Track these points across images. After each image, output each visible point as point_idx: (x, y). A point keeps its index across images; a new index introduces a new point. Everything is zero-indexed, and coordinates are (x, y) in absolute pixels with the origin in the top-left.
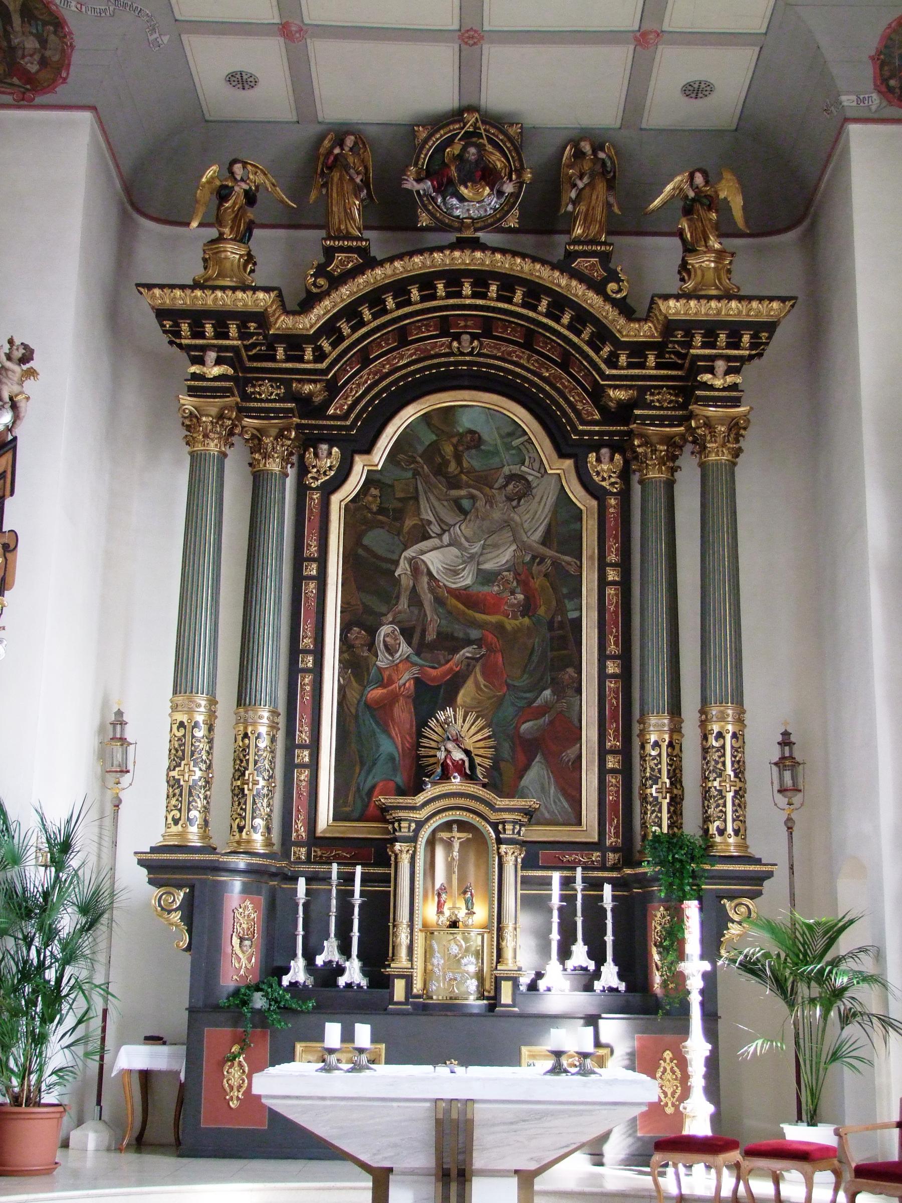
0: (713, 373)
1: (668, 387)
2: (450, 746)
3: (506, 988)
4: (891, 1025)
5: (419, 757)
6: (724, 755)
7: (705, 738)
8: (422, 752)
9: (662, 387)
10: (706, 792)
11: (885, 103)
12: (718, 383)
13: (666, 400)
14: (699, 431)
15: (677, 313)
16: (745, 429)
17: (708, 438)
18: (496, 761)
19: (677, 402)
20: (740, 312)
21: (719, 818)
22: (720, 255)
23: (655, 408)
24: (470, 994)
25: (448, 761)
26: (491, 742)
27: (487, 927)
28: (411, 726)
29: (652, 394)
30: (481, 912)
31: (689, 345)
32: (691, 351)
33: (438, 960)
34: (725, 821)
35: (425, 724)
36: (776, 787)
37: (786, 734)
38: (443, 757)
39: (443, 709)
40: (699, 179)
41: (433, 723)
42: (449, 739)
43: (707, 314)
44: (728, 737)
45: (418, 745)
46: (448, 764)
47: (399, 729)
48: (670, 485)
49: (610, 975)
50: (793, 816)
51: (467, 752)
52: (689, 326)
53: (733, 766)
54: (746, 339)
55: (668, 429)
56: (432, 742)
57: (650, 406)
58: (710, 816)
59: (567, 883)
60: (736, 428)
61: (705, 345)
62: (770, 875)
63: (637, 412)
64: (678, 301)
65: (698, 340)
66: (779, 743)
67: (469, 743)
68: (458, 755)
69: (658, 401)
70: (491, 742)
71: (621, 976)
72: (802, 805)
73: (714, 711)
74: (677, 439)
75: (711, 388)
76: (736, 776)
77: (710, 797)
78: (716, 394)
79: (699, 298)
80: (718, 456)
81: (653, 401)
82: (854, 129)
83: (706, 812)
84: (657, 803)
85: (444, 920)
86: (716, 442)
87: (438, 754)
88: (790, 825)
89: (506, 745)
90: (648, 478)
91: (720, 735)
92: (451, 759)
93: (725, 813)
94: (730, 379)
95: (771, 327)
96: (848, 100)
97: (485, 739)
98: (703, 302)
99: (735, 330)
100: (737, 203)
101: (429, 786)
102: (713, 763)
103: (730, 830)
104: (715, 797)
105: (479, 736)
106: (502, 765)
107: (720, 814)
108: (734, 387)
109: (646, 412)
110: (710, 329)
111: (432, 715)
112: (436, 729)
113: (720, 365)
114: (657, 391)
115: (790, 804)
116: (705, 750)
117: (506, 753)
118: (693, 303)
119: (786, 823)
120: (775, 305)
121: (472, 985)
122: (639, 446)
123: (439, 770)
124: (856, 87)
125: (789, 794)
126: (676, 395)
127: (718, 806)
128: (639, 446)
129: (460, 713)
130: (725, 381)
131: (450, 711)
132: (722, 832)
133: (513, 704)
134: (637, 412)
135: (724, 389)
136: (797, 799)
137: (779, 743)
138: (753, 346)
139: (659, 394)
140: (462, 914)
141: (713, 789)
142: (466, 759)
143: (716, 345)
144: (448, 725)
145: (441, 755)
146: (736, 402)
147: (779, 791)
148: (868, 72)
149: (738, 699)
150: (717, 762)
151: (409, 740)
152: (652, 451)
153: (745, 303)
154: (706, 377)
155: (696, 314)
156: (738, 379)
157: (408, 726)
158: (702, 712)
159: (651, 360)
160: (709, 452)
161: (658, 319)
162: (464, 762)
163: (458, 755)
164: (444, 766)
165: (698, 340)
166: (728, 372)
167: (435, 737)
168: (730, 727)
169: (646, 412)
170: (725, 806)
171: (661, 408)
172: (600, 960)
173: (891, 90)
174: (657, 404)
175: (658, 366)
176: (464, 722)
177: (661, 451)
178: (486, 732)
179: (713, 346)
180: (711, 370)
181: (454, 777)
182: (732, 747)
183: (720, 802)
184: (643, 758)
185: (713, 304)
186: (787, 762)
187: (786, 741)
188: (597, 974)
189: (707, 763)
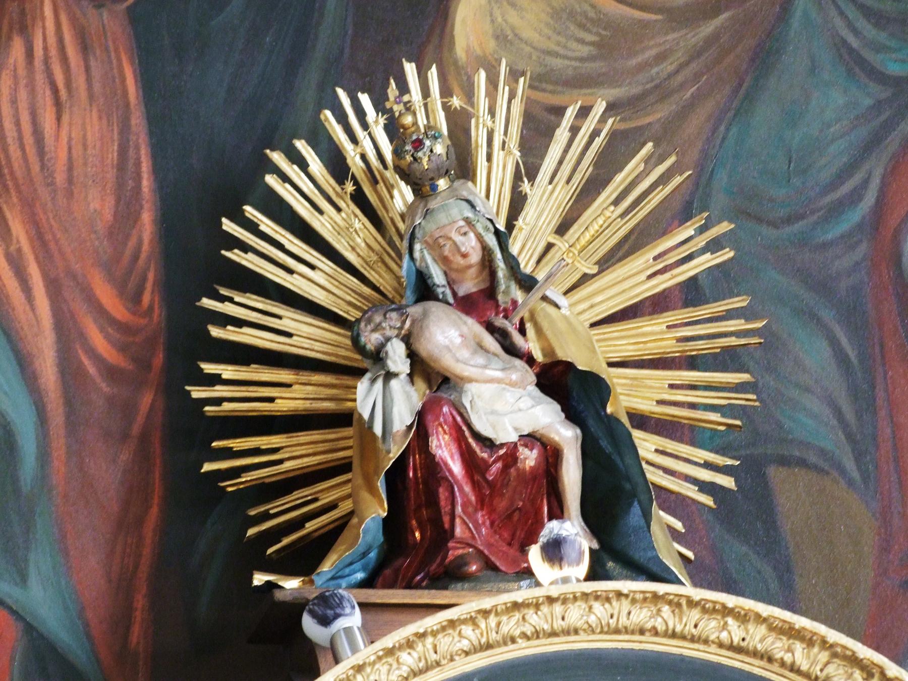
2: (450, 336)
5: (196, 431)
8: (226, 389)
18: (756, 450)
25: (443, 448)
26: (725, 323)
28: (126, 215)
35: (239, 184)
38: (403, 416)
39: (377, 77)
41: (298, 179)
42: (424, 290)
45: (190, 343)
46: (433, 469)
47: (40, 239)
51: (560, 381)
56: (291, 319)
67: (570, 326)
68: (509, 408)
70: (725, 323)
87: (366, 396)
89: (813, 356)
92: (466, 436)
97: (692, 293)
101: (353, 619)
105: (634, 280)
106: (790, 491)
111: (275, 121)
112: (321, 225)
117: (813, 421)
123: (376, 511)
129: (496, 126)
131: (421, 96)
133: (855, 64)
142: (567, 437)
144: (423, 188)
145: (390, 404)
151: (111, 315)
157: (97, 204)
162: (552, 456)
163: (509, 408)
164: (413, 485)
167: (316, 281)
176: (528, 170)
178: (691, 249)
181: (555, 551)
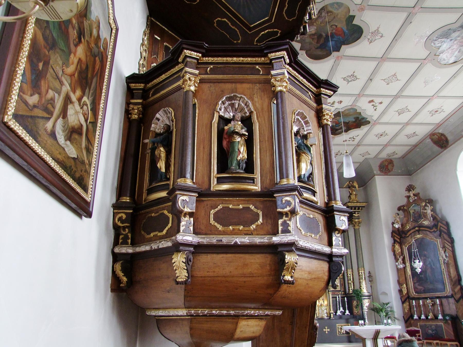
3: (332, 315)
7: (359, 273)
22: (356, 195)
24: (325, 316)
27: (327, 305)
30: (326, 303)
33: (320, 311)
40: (351, 183)
49: (347, 312)
59: (339, 298)
60: (359, 223)
71: (349, 312)
80: (357, 227)
82: (376, 176)
84: (351, 284)
85: (320, 304)
95: (364, 207)
96: (375, 172)
100: (357, 186)
108: (358, 216)
113: (356, 213)
116: (359, 275)
121: (326, 315)
124: (376, 170)
140: (323, 303)
148: (378, 168)
149: (364, 267)
154: (354, 215)
158: (358, 269)
166: (358, 213)
172: (345, 310)
180: (355, 213)
184: (348, 276)
186: (370, 276)
187: (369, 273)
188: (345, 312)
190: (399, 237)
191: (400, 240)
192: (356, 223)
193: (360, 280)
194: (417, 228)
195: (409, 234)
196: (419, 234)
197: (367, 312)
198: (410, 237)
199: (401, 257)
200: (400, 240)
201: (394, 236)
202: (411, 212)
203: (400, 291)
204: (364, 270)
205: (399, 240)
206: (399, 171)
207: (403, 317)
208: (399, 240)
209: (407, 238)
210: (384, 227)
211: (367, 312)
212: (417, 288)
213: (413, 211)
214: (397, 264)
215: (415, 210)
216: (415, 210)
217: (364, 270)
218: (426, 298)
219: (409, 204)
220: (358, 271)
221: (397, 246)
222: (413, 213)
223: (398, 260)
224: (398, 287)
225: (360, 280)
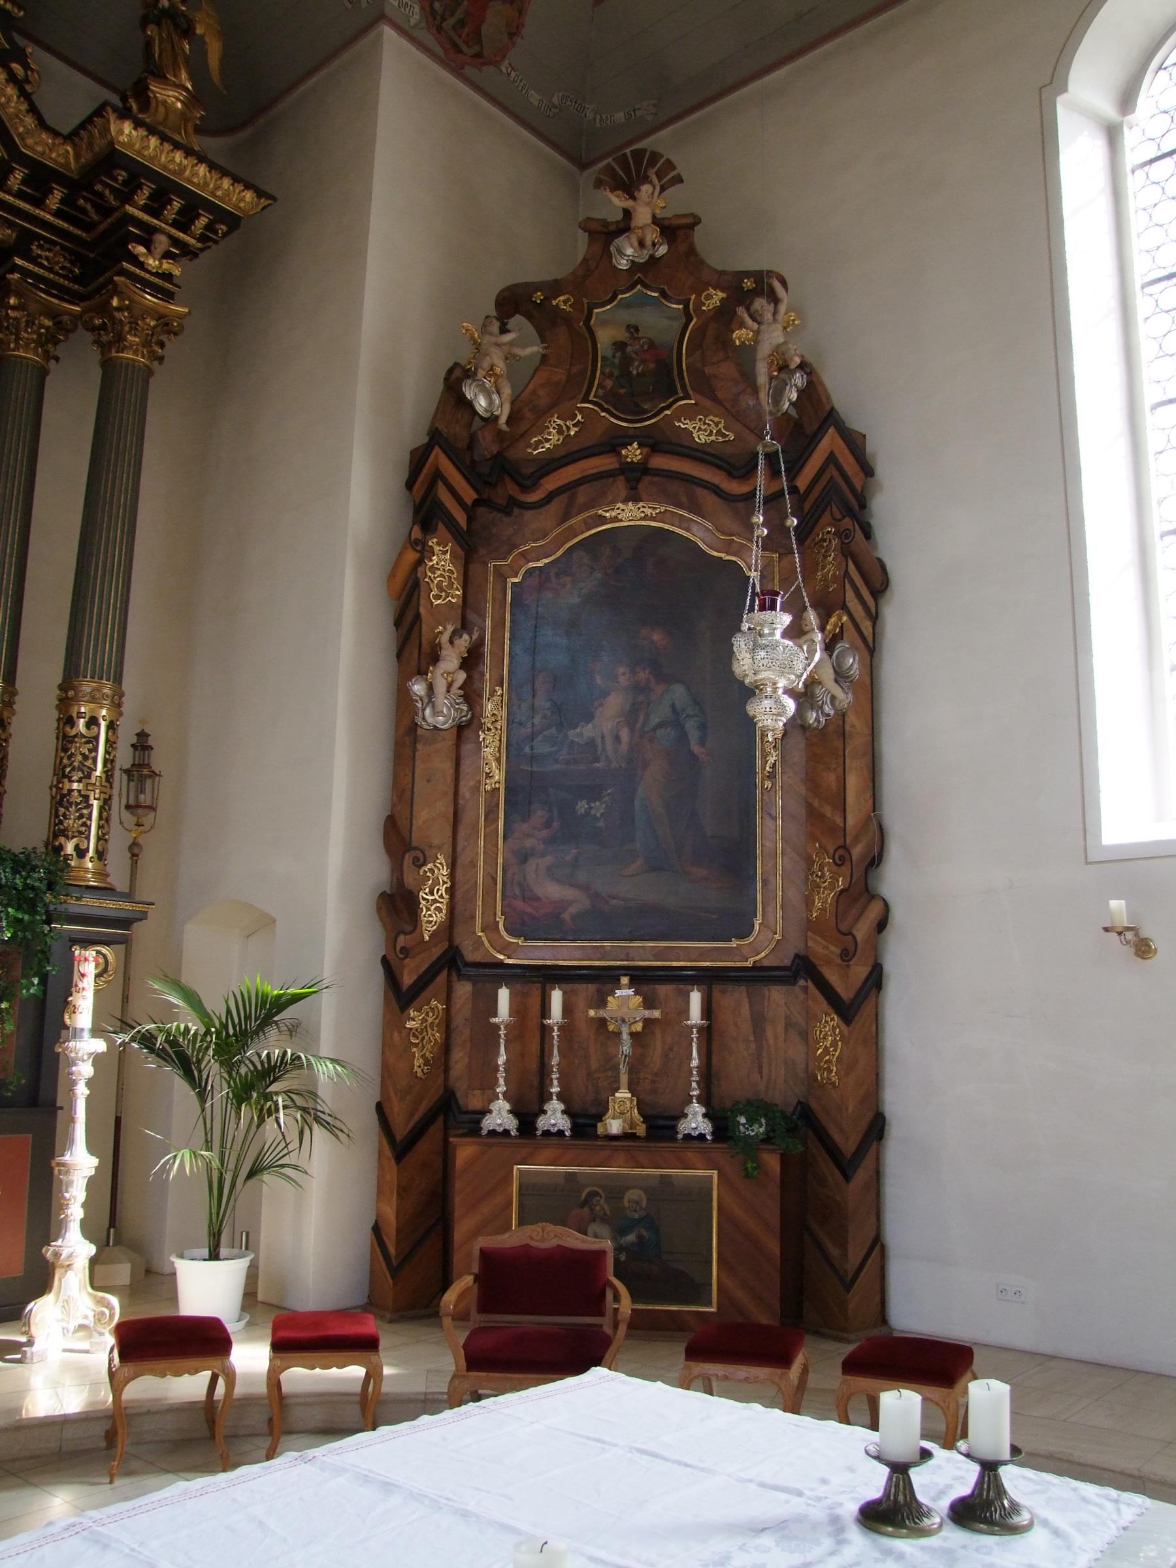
0: (148, 248)
1: (63, 248)
4: (317, 1119)
6: (96, 749)
7: (71, 722)
9: (55, 243)
10: (63, 796)
11: (423, 24)
12: (152, 263)
13: (58, 263)
14: (118, 315)
15: (130, 145)
16: (175, 334)
17: (127, 328)
19: (72, 272)
20: (206, 184)
21: (81, 833)
23: (42, 266)
29: (41, 247)
31: (128, 199)
32: (127, 207)
34: (88, 838)
36: (124, 802)
37: (142, 735)
43: (165, 168)
44: (103, 724)
48: (43, 373)
50: (140, 840)
52: (138, 172)
53: (105, 765)
54: (203, 221)
55: (56, 301)
57: (34, 260)
58: (66, 829)
61: (144, 209)
62: (143, 916)
63: (19, 261)
64: (135, 129)
65: (142, 198)
66: (133, 746)
69: (47, 259)
72: (152, 827)
73: (87, 686)
74: (66, 318)
75: (141, 265)
76: (107, 780)
77: (71, 804)
78: (147, 276)
79: (164, 138)
81: (40, 256)
83: (61, 822)
86: (135, 335)
88: (136, 851)
90: (15, 356)
91: (93, 722)
93: (89, 828)
94: (166, 265)
95: (233, 221)
98: (167, 147)
99: (194, 205)
102: (80, 758)
103: (91, 853)
104: (77, 804)
107: (83, 829)
108: (168, 277)
109: (31, 267)
110: (165, 189)
114: (47, 246)
115: (138, 825)
116: (65, 741)
118: (154, 141)
119: (130, 848)
120: (249, 195)
122: (13, 308)
125: (140, 811)
126: (71, 262)
127: (81, 816)
128: (13, 308)
130: (161, 264)
132: (81, 853)
134: (19, 261)
135: (156, 275)
136: (148, 819)
137: (133, 746)
138: (203, 238)
139: (49, 250)
141: (76, 794)
143: (162, 214)
146: (168, 296)
147: (128, 807)
149: (118, 680)
150: (85, 758)
152: (27, 322)
153: (215, 175)
154: (141, 249)
155: (151, 159)
156: (177, 272)
158: (66, 686)
159: (55, 199)
160: (126, 347)
161: (91, 144)
165: (142, 198)
166: (167, 255)
168: (104, 712)
169: (31, 267)
170: (90, 818)
171: (50, 270)
173: (433, 12)
174: (46, 263)
175: (58, 214)
177: (42, 326)
179: (156, 214)
180: (148, 244)
182: (107, 740)
183: (85, 811)
185: (178, 156)
187: (142, 744)
189: (69, 757)
190: (469, 495)
191: (470, 520)
192: (137, 314)
193: (61, 774)
194: (633, 453)
195: (551, 483)
196: (634, 497)
197: (98, 1059)
198: (555, 507)
199: (464, 642)
200: (470, 511)
201: (438, 476)
202: (605, 337)
203: (397, 905)
204: (117, 706)
205: (461, 518)
206: (534, 97)
207: (379, 1107)
208: (461, 518)
209: (528, 514)
210: (363, 392)
211: (98, 1059)
212: (529, 897)
213: (621, 335)
214: (418, 688)
215: (633, 329)
216: (633, 329)
217: (117, 706)
218: (605, 978)
219: (594, 278)
220: (65, 703)
221: (442, 561)
222: (619, 346)
223: (435, 659)
224: (376, 872)
225: (61, 774)
